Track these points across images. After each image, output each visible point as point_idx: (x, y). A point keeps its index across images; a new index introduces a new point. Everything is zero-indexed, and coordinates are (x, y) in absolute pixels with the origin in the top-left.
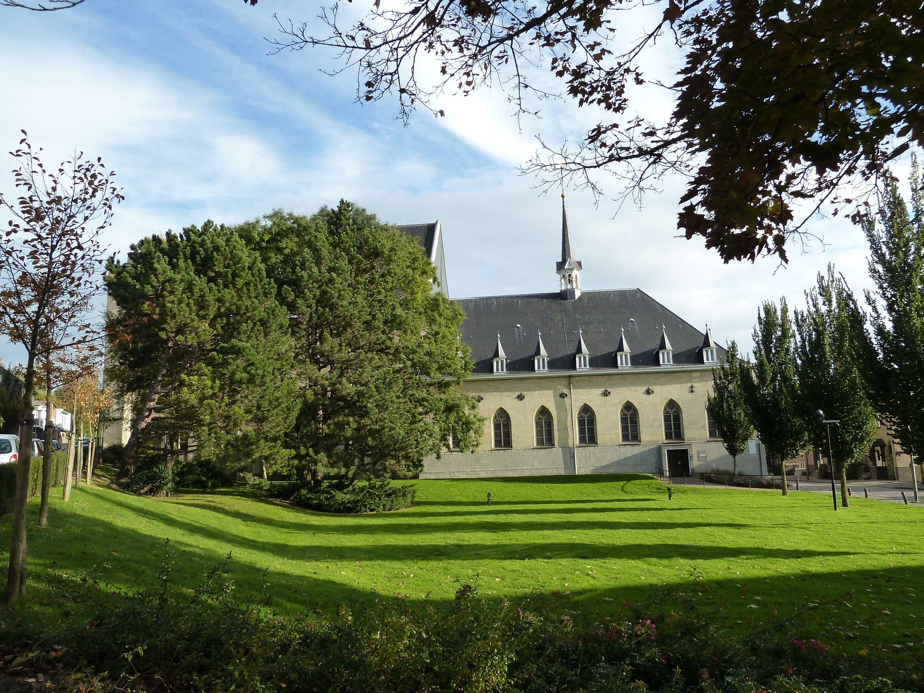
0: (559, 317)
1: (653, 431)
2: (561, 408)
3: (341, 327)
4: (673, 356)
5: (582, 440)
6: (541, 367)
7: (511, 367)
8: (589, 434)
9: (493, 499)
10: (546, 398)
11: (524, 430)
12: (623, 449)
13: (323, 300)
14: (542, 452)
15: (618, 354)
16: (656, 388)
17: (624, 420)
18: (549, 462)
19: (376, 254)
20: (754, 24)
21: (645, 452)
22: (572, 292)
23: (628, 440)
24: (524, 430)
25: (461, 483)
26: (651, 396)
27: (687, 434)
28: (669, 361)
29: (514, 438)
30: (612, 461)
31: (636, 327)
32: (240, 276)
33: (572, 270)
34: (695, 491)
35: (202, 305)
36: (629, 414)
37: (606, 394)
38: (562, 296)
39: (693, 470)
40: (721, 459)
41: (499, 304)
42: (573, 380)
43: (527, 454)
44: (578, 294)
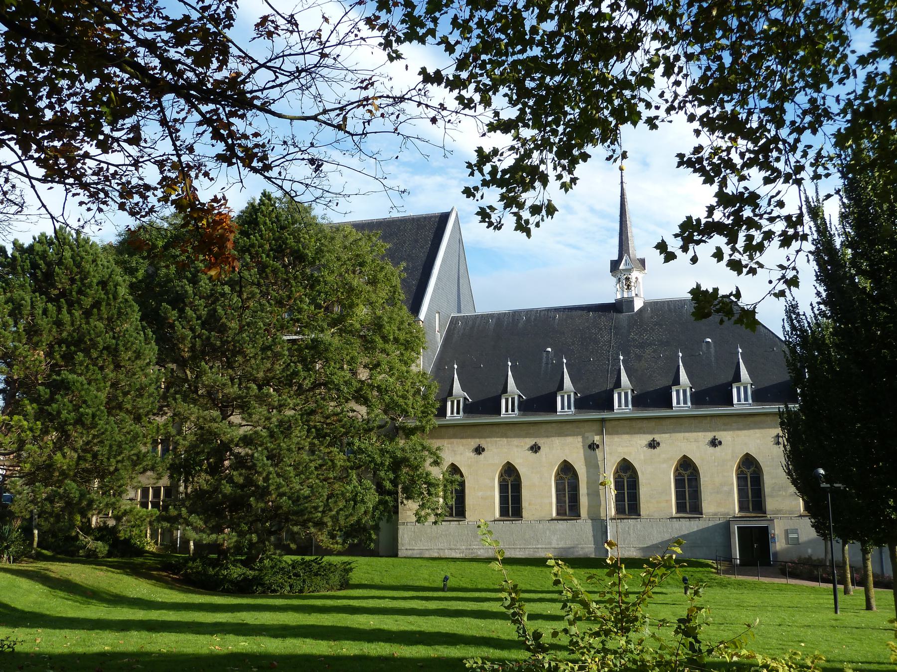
0: (606, 338)
1: (721, 499)
2: (593, 466)
3: (228, 354)
4: (753, 393)
5: (620, 510)
6: (564, 407)
7: (525, 407)
8: (629, 501)
9: (450, 583)
10: (569, 449)
11: (540, 494)
12: (676, 524)
13: (212, 322)
14: (562, 525)
15: (674, 388)
16: (724, 436)
17: (679, 483)
18: (578, 536)
19: (299, 257)
20: (198, 48)
21: (707, 529)
22: (630, 302)
23: (685, 511)
24: (540, 494)
25: (444, 563)
26: (718, 448)
27: (771, 504)
28: (746, 399)
29: (525, 504)
30: (660, 540)
31: (712, 350)
32: (86, 295)
33: (629, 271)
34: (740, 584)
35: (32, 331)
36: (686, 474)
37: (653, 445)
38: (620, 307)
39: (776, 554)
40: (810, 542)
41: (528, 320)
42: (608, 424)
43: (543, 528)
44: (638, 305)
